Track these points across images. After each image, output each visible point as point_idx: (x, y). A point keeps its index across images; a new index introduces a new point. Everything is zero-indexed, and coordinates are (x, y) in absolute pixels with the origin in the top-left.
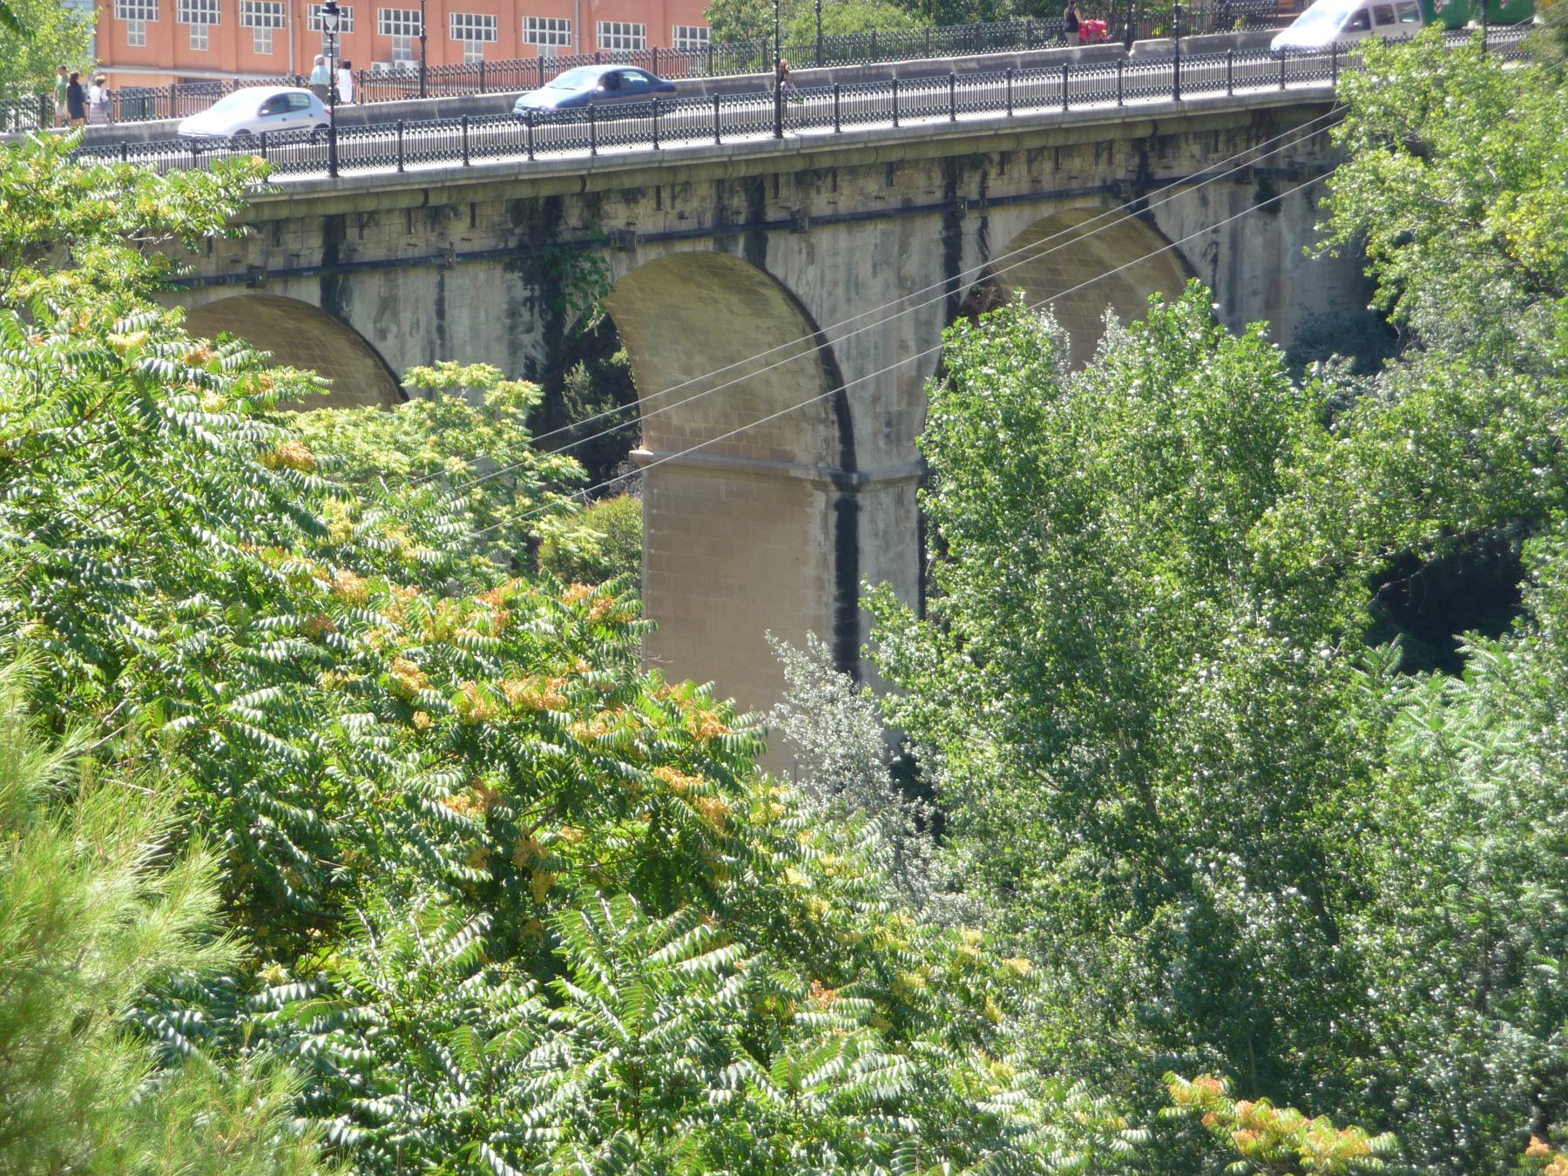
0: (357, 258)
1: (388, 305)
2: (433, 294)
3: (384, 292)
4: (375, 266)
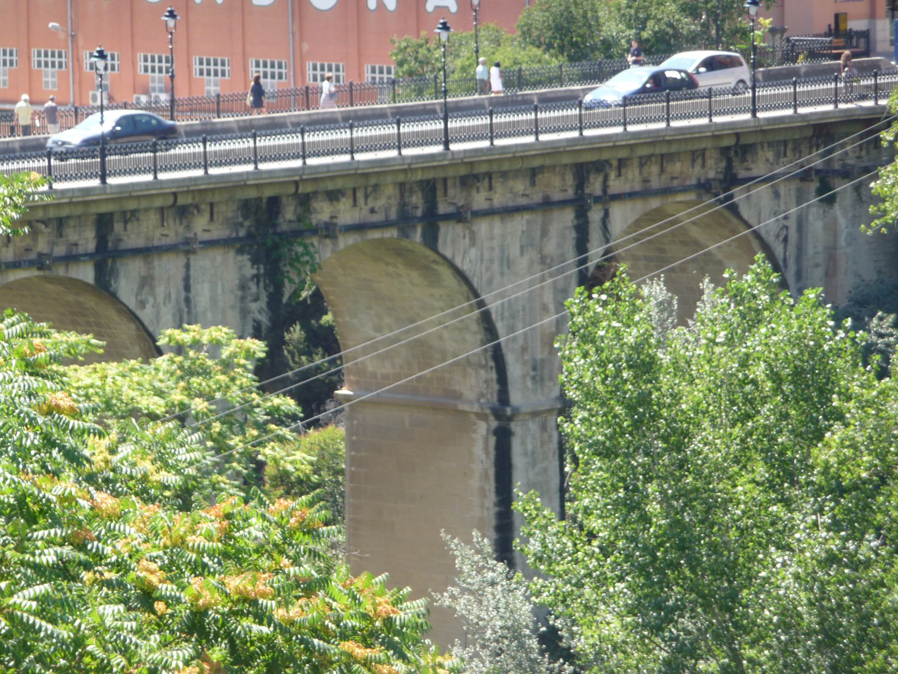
0: (122, 246)
1: (146, 282)
2: (181, 273)
3: (143, 272)
4: (136, 252)
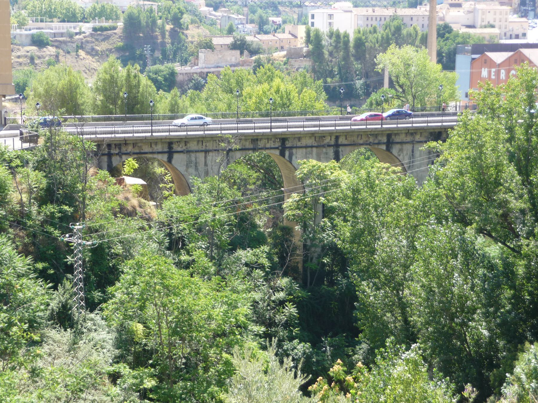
0: (394, 141)
1: (401, 150)
